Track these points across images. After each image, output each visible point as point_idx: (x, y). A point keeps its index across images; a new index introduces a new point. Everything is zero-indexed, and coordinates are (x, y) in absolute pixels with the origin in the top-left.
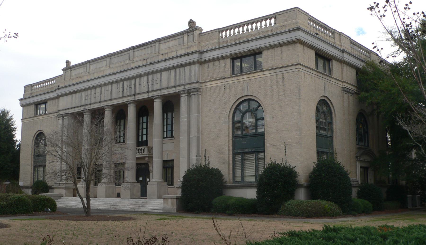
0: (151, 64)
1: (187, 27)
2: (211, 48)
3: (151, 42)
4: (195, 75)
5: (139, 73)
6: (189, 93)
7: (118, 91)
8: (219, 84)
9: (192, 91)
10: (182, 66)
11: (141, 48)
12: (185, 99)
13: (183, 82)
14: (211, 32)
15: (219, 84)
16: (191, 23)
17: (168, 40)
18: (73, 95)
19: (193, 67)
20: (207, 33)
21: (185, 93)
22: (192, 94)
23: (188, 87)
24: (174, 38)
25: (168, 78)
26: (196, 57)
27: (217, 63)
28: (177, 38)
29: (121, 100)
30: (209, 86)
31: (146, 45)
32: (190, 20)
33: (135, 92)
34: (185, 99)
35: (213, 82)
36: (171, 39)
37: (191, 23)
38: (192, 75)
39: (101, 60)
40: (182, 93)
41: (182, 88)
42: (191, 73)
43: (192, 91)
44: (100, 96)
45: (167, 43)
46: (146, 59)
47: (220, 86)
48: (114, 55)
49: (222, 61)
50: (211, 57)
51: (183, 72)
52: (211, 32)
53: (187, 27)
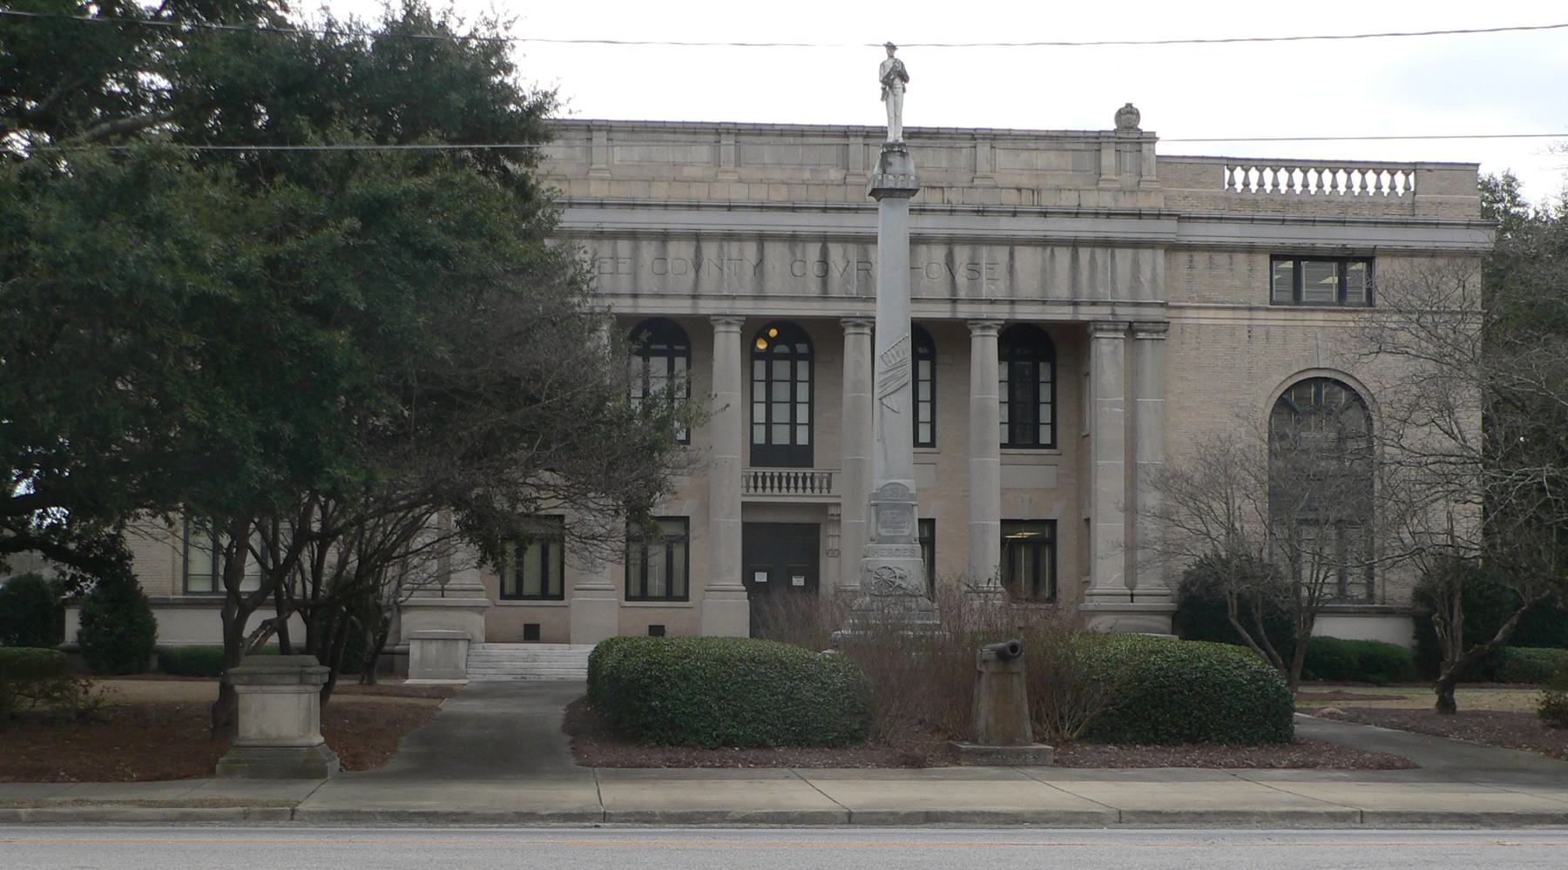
0: (981, 212)
1: (1110, 125)
2: (1217, 214)
4: (1154, 280)
5: (919, 231)
6: (1132, 330)
7: (797, 272)
8: (1231, 322)
9: (1146, 327)
10: (1109, 244)
12: (1116, 347)
13: (1105, 293)
14: (1199, 161)
15: (1231, 322)
16: (1128, 116)
17: (1032, 145)
19: (1146, 255)
20: (1185, 160)
21: (1116, 330)
22: (1141, 335)
23: (1126, 313)
25: (1044, 271)
26: (1166, 230)
27: (1222, 259)
29: (816, 305)
30: (1195, 321)
31: (930, 138)
32: (1129, 105)
34: (1116, 347)
35: (1211, 313)
36: (1041, 145)
37: (1128, 116)
38: (1142, 279)
39: (683, 137)
40: (1105, 327)
41: (1102, 312)
42: (1139, 272)
43: (1146, 328)
44: (692, 274)
45: (1025, 155)
46: (942, 188)
47: (1233, 328)
48: (760, 134)
49: (1241, 258)
50: (1210, 239)
51: (1105, 262)
52: (1199, 161)
53: (1110, 125)
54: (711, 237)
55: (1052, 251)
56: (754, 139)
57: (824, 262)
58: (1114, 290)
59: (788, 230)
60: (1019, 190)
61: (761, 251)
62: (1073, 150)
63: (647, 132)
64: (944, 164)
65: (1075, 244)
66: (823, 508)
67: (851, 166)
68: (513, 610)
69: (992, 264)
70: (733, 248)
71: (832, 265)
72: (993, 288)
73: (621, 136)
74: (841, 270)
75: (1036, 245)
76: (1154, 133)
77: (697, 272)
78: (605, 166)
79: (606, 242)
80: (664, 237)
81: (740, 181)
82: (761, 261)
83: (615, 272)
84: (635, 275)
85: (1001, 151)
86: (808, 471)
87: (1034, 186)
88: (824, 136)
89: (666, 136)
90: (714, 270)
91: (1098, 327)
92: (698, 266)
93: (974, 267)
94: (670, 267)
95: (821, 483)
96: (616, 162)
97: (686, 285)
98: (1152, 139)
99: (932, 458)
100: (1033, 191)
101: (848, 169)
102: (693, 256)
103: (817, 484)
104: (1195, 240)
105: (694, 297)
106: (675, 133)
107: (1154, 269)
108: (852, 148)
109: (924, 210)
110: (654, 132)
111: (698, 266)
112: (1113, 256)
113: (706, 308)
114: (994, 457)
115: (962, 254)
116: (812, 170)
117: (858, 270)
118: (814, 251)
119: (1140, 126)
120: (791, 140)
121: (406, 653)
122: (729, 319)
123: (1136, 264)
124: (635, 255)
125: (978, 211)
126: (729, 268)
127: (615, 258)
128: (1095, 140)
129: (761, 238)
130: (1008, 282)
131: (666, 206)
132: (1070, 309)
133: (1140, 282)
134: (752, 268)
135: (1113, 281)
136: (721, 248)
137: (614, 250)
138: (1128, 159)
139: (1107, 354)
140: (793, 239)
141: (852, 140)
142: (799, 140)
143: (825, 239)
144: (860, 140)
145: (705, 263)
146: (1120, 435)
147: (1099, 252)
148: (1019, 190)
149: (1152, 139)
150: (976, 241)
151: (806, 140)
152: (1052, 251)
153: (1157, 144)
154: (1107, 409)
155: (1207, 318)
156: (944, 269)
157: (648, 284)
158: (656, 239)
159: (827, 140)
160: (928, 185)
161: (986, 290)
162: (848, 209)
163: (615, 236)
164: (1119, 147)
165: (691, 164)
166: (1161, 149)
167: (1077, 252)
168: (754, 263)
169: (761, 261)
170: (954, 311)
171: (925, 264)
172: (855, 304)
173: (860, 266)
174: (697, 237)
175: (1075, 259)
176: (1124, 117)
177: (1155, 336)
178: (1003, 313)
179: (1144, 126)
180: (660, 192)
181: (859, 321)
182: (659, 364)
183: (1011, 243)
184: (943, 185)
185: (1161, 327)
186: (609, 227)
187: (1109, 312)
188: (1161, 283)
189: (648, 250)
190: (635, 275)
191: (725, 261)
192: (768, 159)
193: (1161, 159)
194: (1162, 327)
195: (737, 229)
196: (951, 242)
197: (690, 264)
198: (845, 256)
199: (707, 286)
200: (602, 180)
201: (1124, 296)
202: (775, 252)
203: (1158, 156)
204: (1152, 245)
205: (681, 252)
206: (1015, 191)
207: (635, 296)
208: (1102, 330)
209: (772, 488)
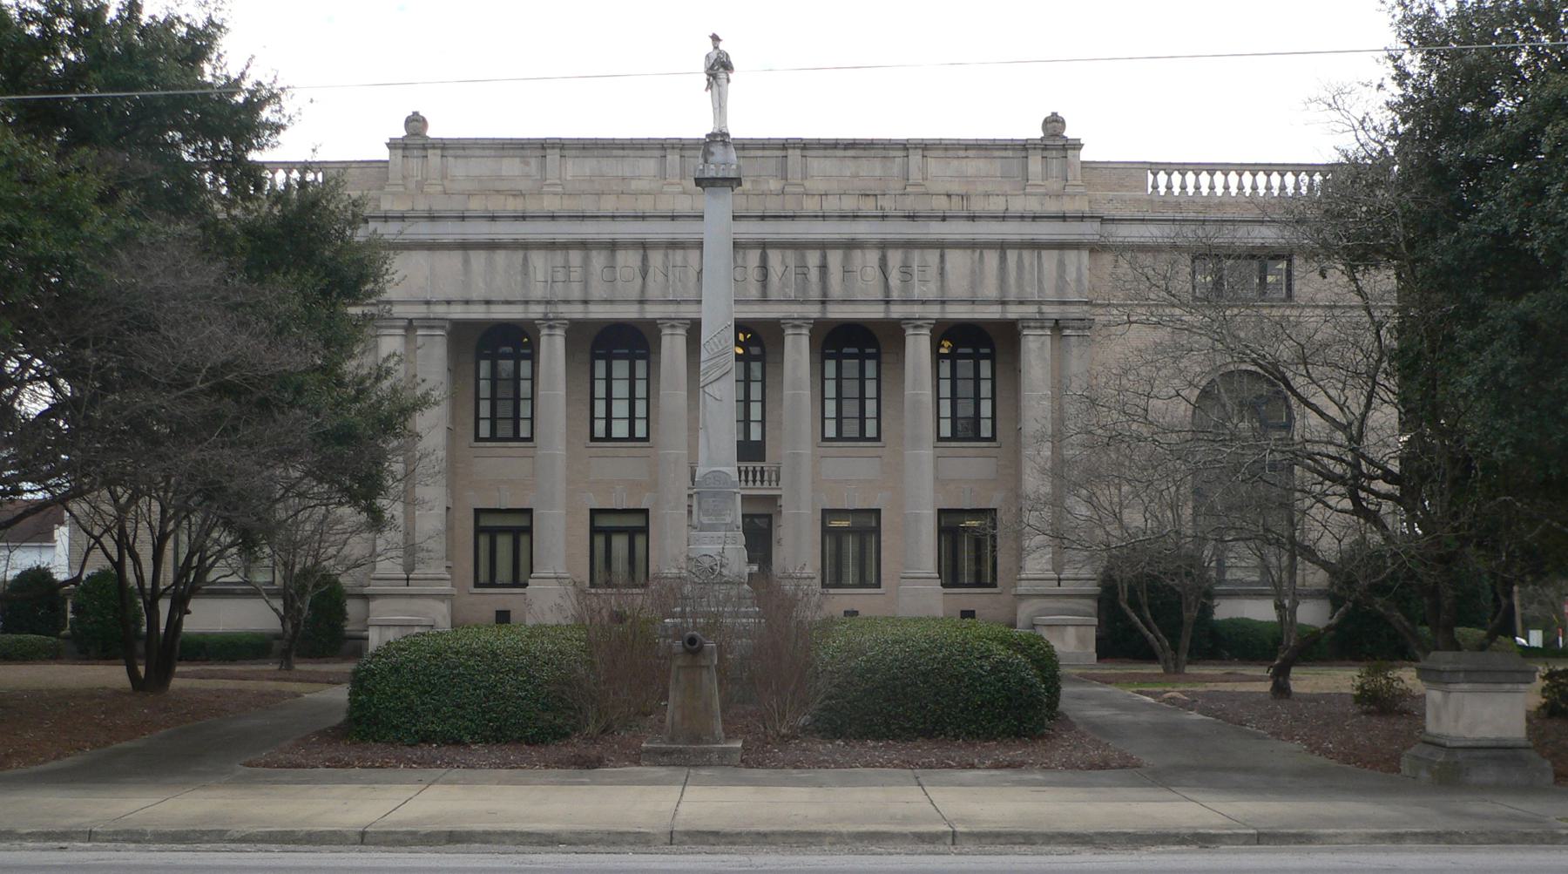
0: (912, 217)
1: (1037, 133)
2: (1140, 215)
4: (1079, 280)
5: (853, 236)
6: (1058, 326)
9: (1071, 324)
10: (1036, 246)
11: (840, 153)
12: (1043, 343)
13: (1031, 292)
16: (1054, 123)
17: (962, 153)
19: (1071, 256)
20: (1110, 166)
21: (1042, 328)
22: (1068, 332)
23: (1052, 312)
24: (983, 153)
25: (973, 272)
26: (1089, 231)
28: (997, 153)
29: (756, 308)
31: (865, 149)
32: (1054, 114)
33: (825, 294)
34: (1043, 343)
36: (971, 153)
37: (1054, 123)
39: (631, 153)
40: (1032, 324)
41: (1030, 311)
44: (639, 281)
45: (955, 163)
46: (876, 195)
51: (1032, 264)
52: (1122, 166)
53: (1037, 133)
54: (656, 245)
55: (981, 253)
57: (764, 266)
58: (1041, 289)
60: (949, 196)
63: (597, 148)
64: (878, 173)
65: (1002, 246)
66: (774, 499)
67: (789, 176)
68: (486, 597)
69: (924, 267)
71: (771, 270)
78: (558, 182)
79: (559, 252)
80: (613, 246)
83: (568, 281)
84: (585, 283)
86: (758, 465)
87: (964, 192)
88: (764, 149)
89: (615, 152)
90: (660, 278)
91: (1025, 324)
92: (644, 274)
93: (906, 270)
95: (770, 477)
97: (633, 291)
98: (1077, 145)
102: (640, 264)
103: (766, 477)
105: (642, 302)
106: (623, 149)
109: (857, 216)
110: (604, 148)
111: (644, 274)
112: (1039, 257)
113: (652, 312)
114: (927, 452)
115: (895, 258)
119: (1065, 134)
121: (367, 639)
122: (674, 323)
123: (1061, 265)
124: (586, 263)
125: (909, 217)
127: (567, 267)
128: (1025, 147)
130: (939, 284)
131: (613, 217)
132: (998, 308)
135: (1040, 281)
136: (666, 256)
137: (567, 261)
138: (1055, 165)
139: (1035, 350)
141: (790, 152)
143: (764, 246)
144: (798, 152)
145: (651, 270)
147: (1026, 254)
148: (949, 196)
149: (1077, 145)
150: (909, 245)
152: (981, 253)
157: (598, 290)
158: (606, 248)
159: (767, 153)
160: (863, 192)
163: (566, 246)
164: (1046, 153)
165: (639, 178)
166: (1086, 155)
167: (1005, 253)
170: (887, 311)
173: (799, 271)
174: (644, 246)
175: (1003, 259)
176: (1049, 126)
177: (1080, 333)
178: (934, 312)
179: (1069, 133)
180: (608, 205)
181: (797, 322)
182: (620, 368)
183: (942, 246)
184: (877, 192)
186: (561, 238)
189: (598, 259)
190: (585, 283)
191: (670, 268)
193: (1088, 166)
196: (884, 246)
199: (654, 291)
200: (556, 194)
201: (1050, 294)
203: (1083, 162)
204: (1076, 246)
205: (628, 260)
206: (945, 198)
207: (586, 302)
208: (1029, 327)
209: (754, 481)
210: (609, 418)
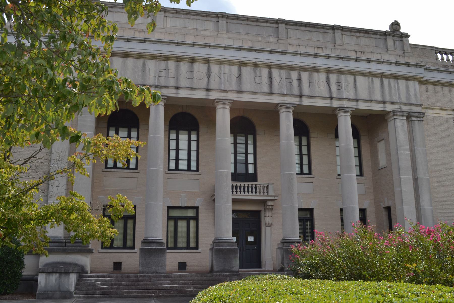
0: (342, 58)
3: (362, 30)
4: (415, 95)
5: (314, 65)
6: (409, 116)
7: (257, 81)
8: (446, 116)
10: (396, 77)
11: (303, 28)
14: (425, 48)
15: (446, 116)
16: (395, 25)
18: (169, 62)
19: (411, 83)
20: (419, 47)
21: (403, 116)
22: (413, 118)
23: (406, 108)
24: (367, 35)
25: (369, 88)
27: (439, 88)
28: (373, 36)
30: (432, 115)
31: (314, 28)
33: (301, 92)
34: (403, 123)
35: (438, 111)
36: (362, 35)
37: (395, 25)
38: (411, 94)
40: (398, 114)
41: (396, 107)
42: (409, 90)
43: (415, 115)
44: (206, 79)
47: (447, 118)
48: (238, 19)
49: (446, 88)
50: (435, 79)
51: (395, 86)
52: (425, 48)
54: (216, 62)
55: (372, 79)
56: (235, 21)
57: (270, 77)
58: (400, 98)
59: (253, 60)
60: (356, 51)
61: (240, 70)
62: (375, 38)
63: (183, 14)
64: (321, 39)
65: (382, 76)
67: (280, 36)
68: (108, 254)
69: (347, 83)
70: (226, 69)
71: (274, 80)
72: (348, 94)
73: (171, 15)
74: (279, 82)
75: (365, 76)
76: (408, 33)
77: (208, 79)
78: (163, 27)
79: (163, 62)
80: (192, 60)
81: (229, 38)
82: (240, 76)
83: (167, 77)
84: (177, 78)
85: (345, 36)
86: (254, 184)
87: (362, 51)
88: (267, 22)
89: (193, 17)
90: (217, 79)
91: (395, 113)
92: (209, 76)
93: (339, 84)
94: (195, 75)
95: (260, 190)
96: (168, 27)
97: (203, 84)
98: (407, 36)
99: (311, 180)
100: (362, 52)
101: (279, 38)
102: (206, 71)
103: (258, 190)
104: (429, 79)
105: (208, 90)
106: (197, 15)
107: (415, 90)
108: (280, 28)
109: (316, 55)
110: (187, 14)
111: (209, 76)
112: (398, 83)
113: (213, 96)
115: (333, 78)
116: (262, 37)
117: (286, 82)
118: (265, 72)
119: (401, 31)
120: (252, 23)
121: (37, 280)
122: (225, 102)
123: (407, 87)
124: (177, 69)
125: (340, 58)
126: (224, 78)
127: (167, 69)
128: (385, 34)
129: (240, 64)
130: (354, 92)
131: (194, 45)
132: (382, 105)
133: (410, 95)
134: (235, 79)
135: (399, 94)
136: (220, 68)
137: (167, 66)
138: (398, 44)
140: (255, 65)
141: (280, 25)
142: (255, 23)
143: (270, 66)
144: (284, 25)
145: (212, 75)
146: (409, 164)
147: (392, 81)
148: (356, 51)
149: (407, 36)
150: (340, 72)
151: (258, 24)
152: (372, 79)
153: (409, 38)
154: (402, 152)
155: (437, 113)
156: (326, 84)
157: (184, 83)
158: (188, 62)
159: (268, 25)
160: (316, 46)
161: (345, 95)
162: (282, 52)
163: (167, 58)
164: (394, 38)
165: (205, 30)
166: (411, 41)
167: (382, 80)
168: (237, 76)
169: (240, 76)
170: (331, 103)
171: (317, 82)
172: (285, 98)
173: (288, 80)
174: (208, 61)
175: (382, 83)
176: (394, 26)
177: (419, 119)
178: (353, 105)
179: (403, 30)
180: (190, 39)
181: (288, 106)
182: (183, 136)
183: (355, 73)
184: (322, 47)
185: (421, 115)
186: (165, 53)
187: (399, 108)
188: (419, 96)
189: (184, 67)
190: (177, 78)
191: (222, 74)
192: (241, 31)
193: (413, 46)
194: (422, 115)
195: (229, 58)
196: (328, 71)
197: (205, 75)
198: (280, 75)
199: (214, 85)
200: (161, 33)
201: (404, 100)
202: (247, 71)
203: (410, 44)
204: (413, 79)
205: (200, 68)
206: (354, 53)
207: (177, 88)
208: (397, 115)
210: (177, 160)
